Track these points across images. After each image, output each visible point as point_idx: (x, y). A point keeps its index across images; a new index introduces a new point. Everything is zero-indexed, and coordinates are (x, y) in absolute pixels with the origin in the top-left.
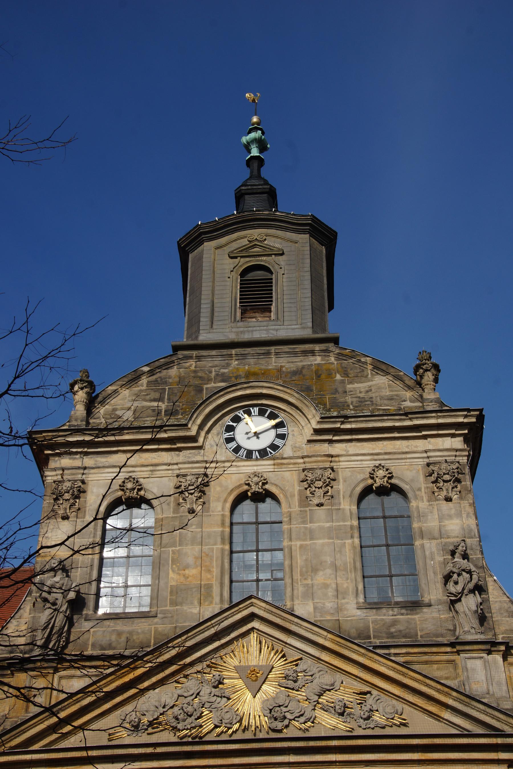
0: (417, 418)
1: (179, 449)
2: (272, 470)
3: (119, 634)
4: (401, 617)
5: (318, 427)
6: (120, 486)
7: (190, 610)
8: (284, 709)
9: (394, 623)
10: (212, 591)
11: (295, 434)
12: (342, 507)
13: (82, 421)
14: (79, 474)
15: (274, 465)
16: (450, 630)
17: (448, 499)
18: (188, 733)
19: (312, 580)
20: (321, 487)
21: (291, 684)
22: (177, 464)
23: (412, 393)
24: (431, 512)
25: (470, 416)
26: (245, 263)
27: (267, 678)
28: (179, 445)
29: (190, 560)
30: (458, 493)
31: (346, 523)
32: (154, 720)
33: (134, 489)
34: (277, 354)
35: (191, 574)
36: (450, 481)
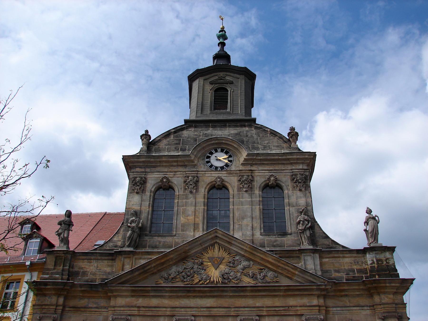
2: (226, 176)
4: (279, 238)
6: (161, 180)
7: (190, 234)
8: (229, 275)
9: (276, 241)
10: (199, 226)
11: (236, 160)
12: (255, 192)
13: (145, 152)
14: (143, 174)
15: (227, 173)
16: (298, 244)
18: (188, 283)
19: (242, 222)
20: (247, 184)
21: (231, 265)
22: (185, 172)
24: (293, 195)
26: (217, 86)
27: (221, 262)
29: (190, 213)
30: (304, 188)
31: (257, 199)
32: (174, 277)
35: (190, 219)
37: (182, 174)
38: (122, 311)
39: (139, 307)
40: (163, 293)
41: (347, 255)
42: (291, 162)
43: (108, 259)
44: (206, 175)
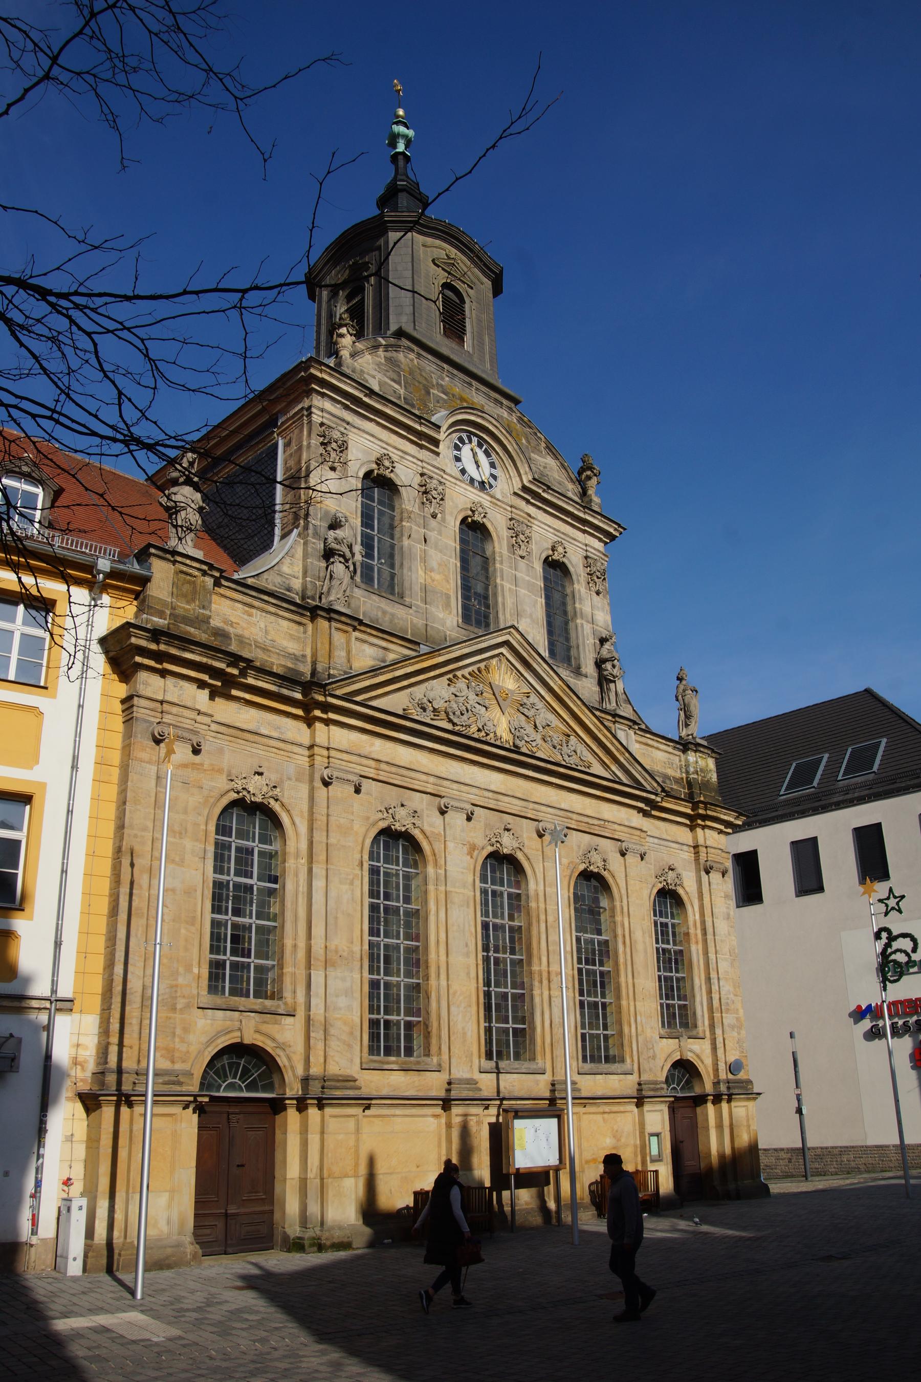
0: (589, 514)
1: (421, 447)
3: (384, 613)
5: (527, 484)
15: (491, 502)
17: (598, 593)
23: (573, 487)
25: (617, 530)
28: (423, 443)
29: (434, 564)
33: (388, 468)
34: (477, 389)
36: (600, 578)
38: (344, 763)
43: (289, 620)
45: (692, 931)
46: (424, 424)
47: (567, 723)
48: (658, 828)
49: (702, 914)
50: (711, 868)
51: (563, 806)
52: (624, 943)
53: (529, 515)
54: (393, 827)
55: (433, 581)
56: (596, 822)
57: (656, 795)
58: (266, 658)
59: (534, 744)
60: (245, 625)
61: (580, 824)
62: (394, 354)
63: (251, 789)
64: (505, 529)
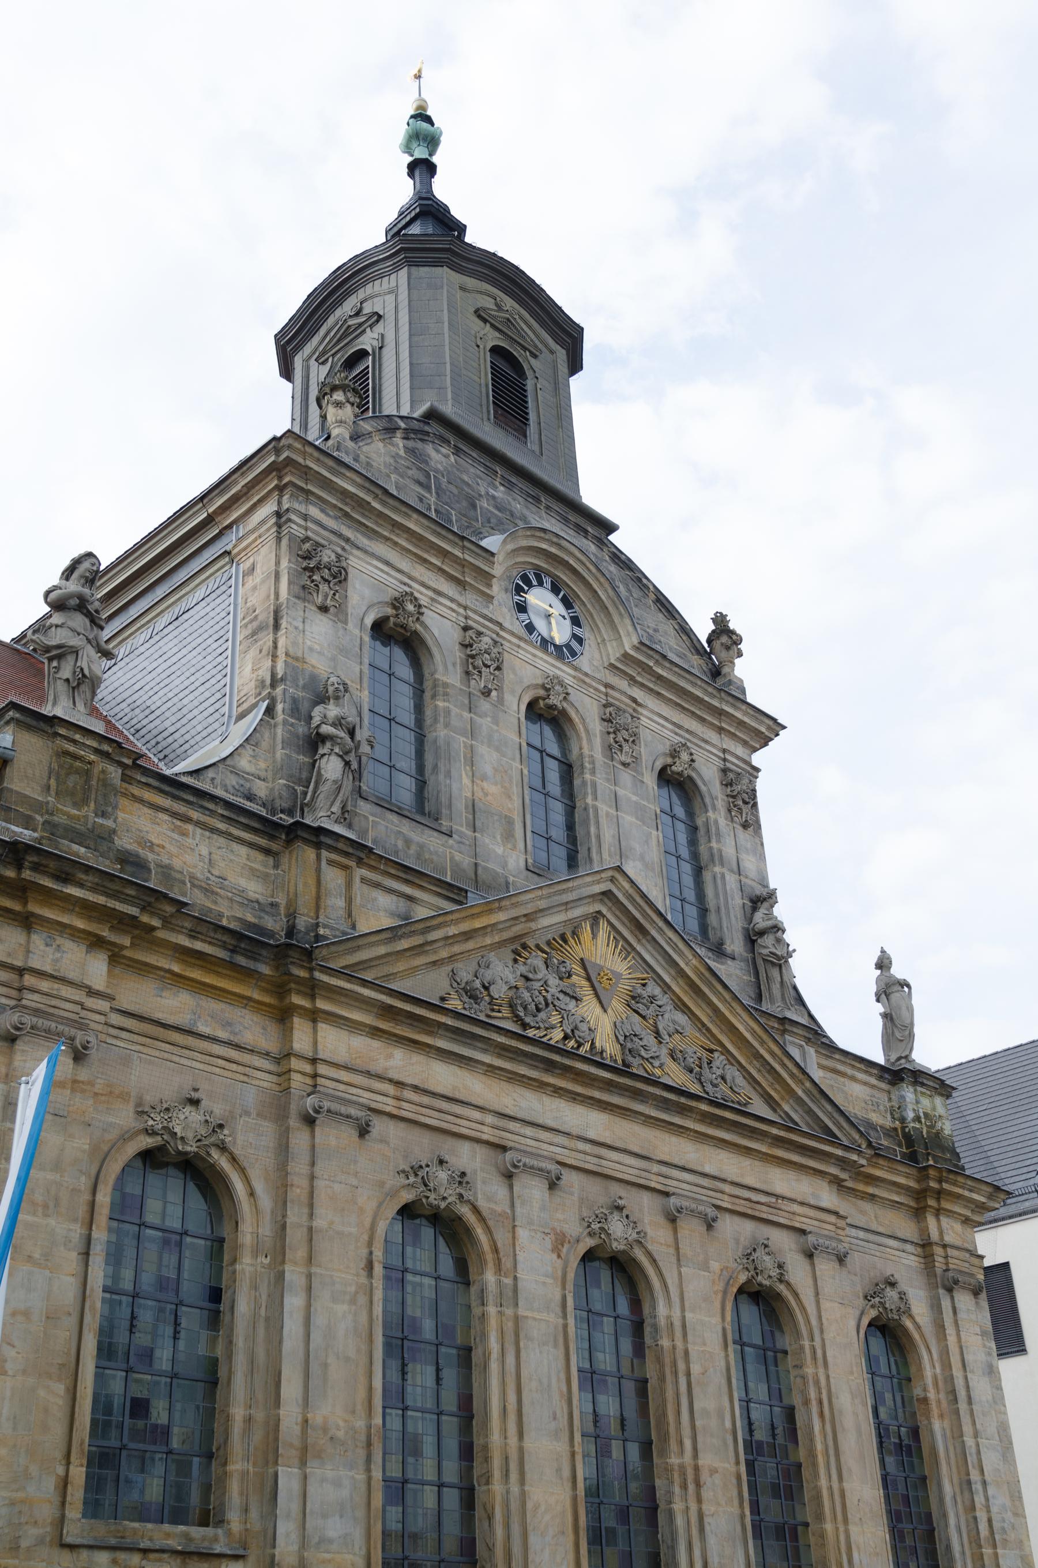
3: (408, 842)
5: (632, 652)
12: (645, 780)
15: (574, 677)
29: (488, 769)
34: (548, 508)
37: (453, 610)
38: (342, 1087)
39: (399, 1084)
40: (475, 1048)
41: (861, 1076)
42: (724, 725)
43: (251, 845)
44: (520, 651)
45: (932, 1395)
46: (469, 549)
47: (708, 1030)
48: (863, 1213)
49: (947, 1365)
50: (956, 1282)
51: (708, 1169)
52: (821, 1415)
53: (634, 700)
54: (424, 1200)
55: (486, 795)
56: (763, 1199)
57: (860, 1153)
58: (210, 905)
59: (657, 1063)
60: (173, 850)
61: (737, 1201)
62: (419, 445)
63: (178, 1130)
64: (597, 721)
